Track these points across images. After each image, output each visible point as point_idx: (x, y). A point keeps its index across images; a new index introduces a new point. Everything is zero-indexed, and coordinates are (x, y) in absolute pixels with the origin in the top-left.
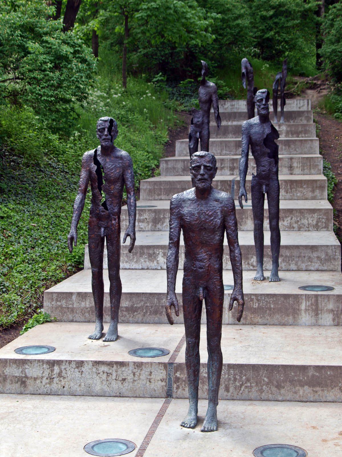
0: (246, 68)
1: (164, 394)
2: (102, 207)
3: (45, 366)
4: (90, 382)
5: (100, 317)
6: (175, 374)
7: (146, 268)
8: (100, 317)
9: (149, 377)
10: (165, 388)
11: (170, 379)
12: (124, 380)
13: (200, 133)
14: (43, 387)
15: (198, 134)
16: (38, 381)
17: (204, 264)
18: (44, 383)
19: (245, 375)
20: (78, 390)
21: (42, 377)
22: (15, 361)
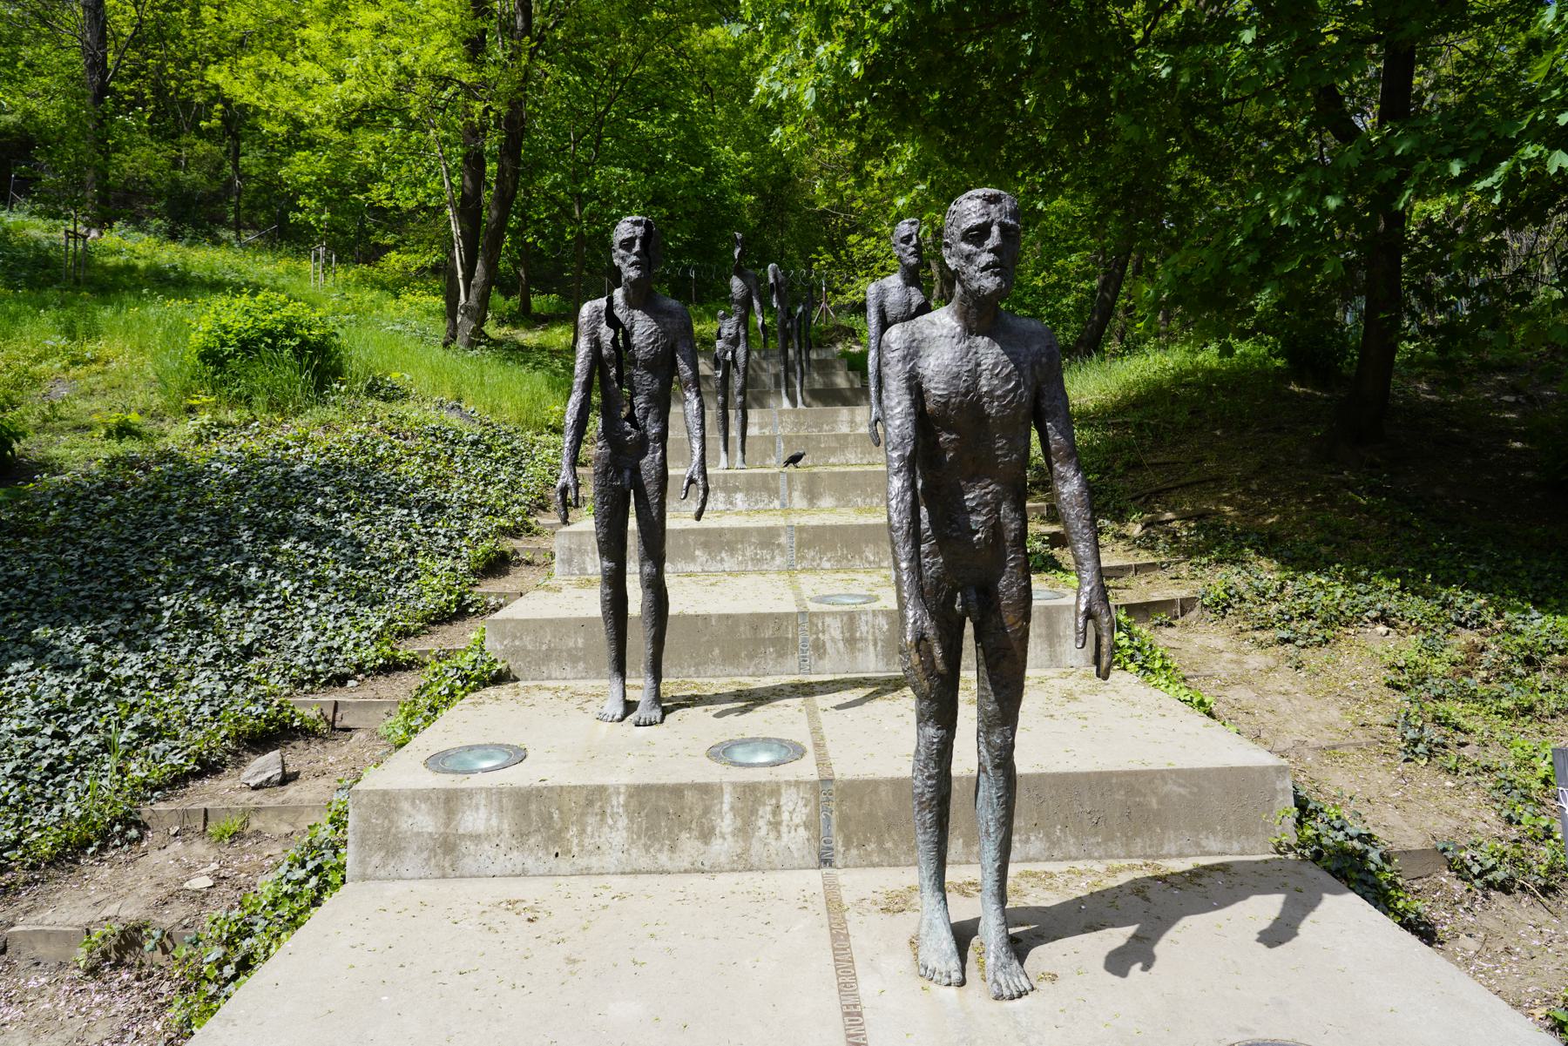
0: (775, 277)
1: (813, 859)
5: (620, 667)
8: (620, 667)
13: (734, 353)
14: (502, 857)
22: (424, 796)
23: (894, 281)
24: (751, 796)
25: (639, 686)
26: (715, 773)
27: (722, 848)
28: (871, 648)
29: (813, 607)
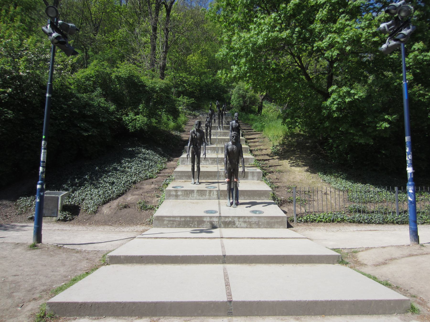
22: (174, 190)
23: (234, 122)
24: (210, 191)
25: (197, 181)
26: (206, 189)
27: (207, 197)
29: (220, 170)
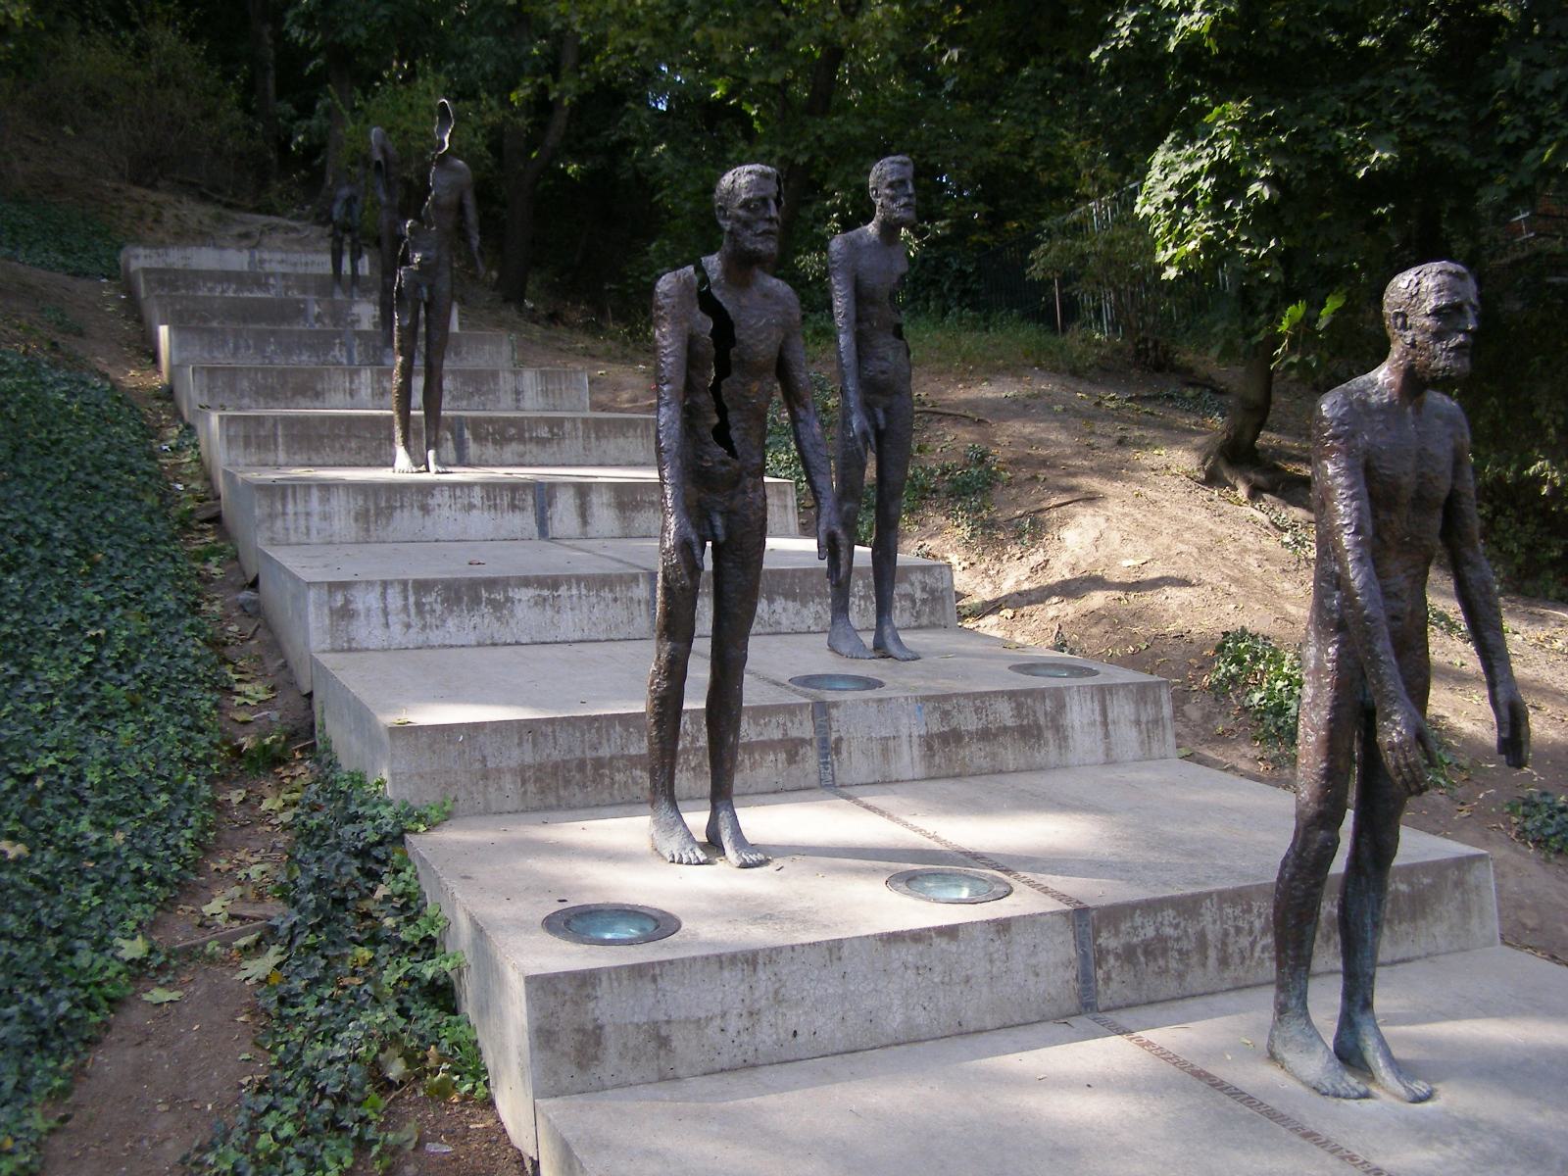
2: (721, 449)
3: (726, 974)
4: (869, 1003)
6: (1095, 939)
7: (489, 642)
9: (1033, 961)
10: (1077, 986)
11: (1085, 956)
12: (967, 980)
13: (431, 288)
15: (425, 290)
16: (711, 1031)
17: (1403, 605)
18: (732, 1032)
19: (1260, 915)
20: (839, 1035)
21: (724, 1015)
28: (905, 747)
